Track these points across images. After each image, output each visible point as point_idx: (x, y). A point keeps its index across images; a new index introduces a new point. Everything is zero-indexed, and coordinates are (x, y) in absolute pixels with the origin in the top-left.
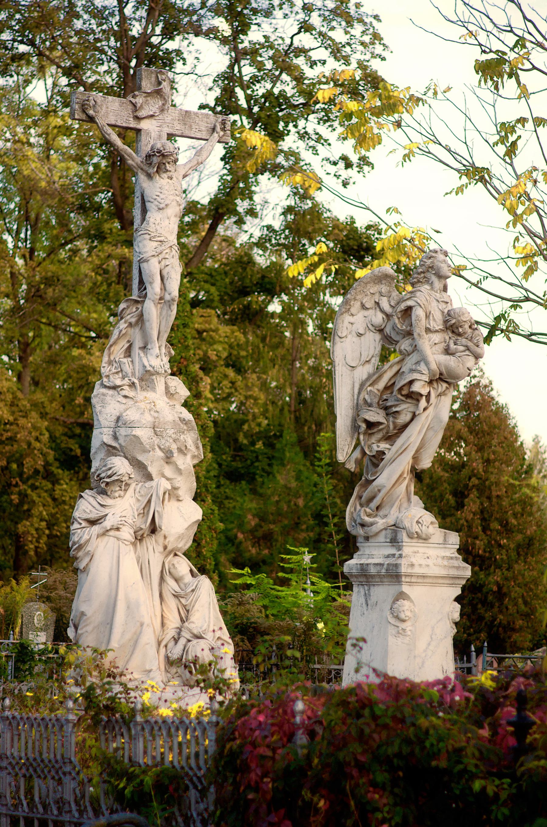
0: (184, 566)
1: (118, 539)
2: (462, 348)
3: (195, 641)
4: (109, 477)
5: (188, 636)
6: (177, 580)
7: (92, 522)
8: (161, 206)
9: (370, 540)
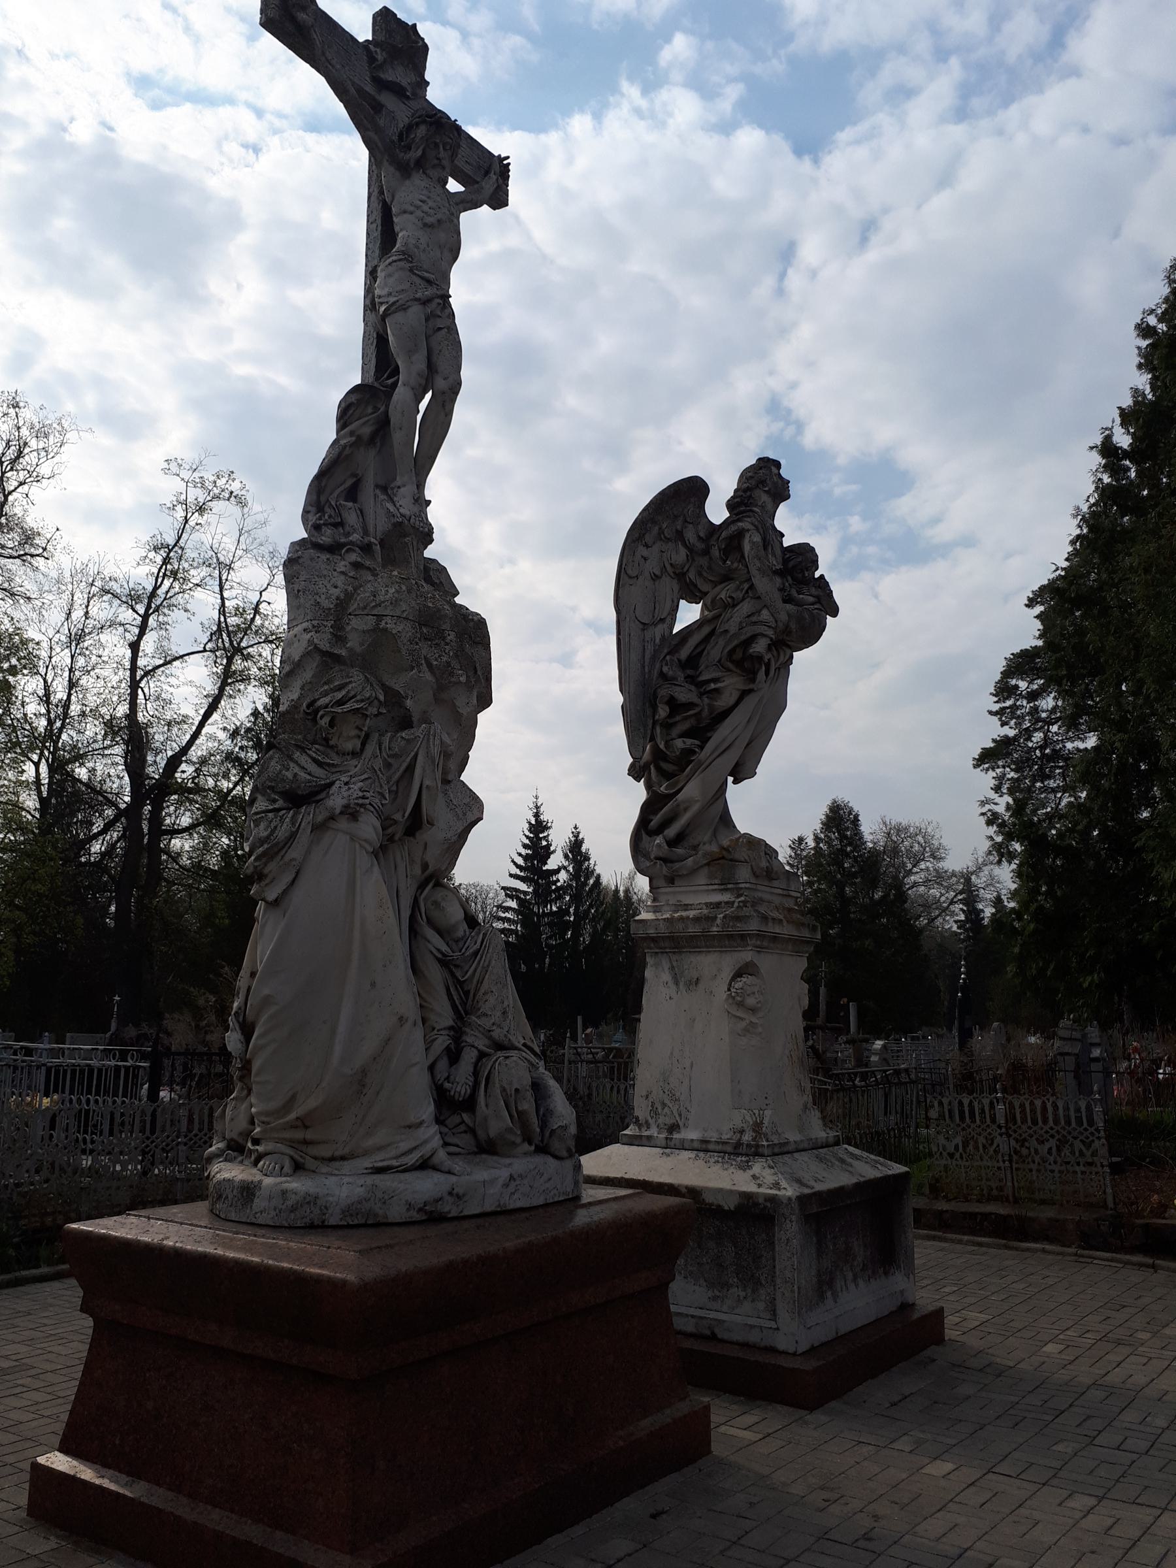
2: (811, 599)
5: (481, 1043)
6: (440, 933)
8: (429, 220)
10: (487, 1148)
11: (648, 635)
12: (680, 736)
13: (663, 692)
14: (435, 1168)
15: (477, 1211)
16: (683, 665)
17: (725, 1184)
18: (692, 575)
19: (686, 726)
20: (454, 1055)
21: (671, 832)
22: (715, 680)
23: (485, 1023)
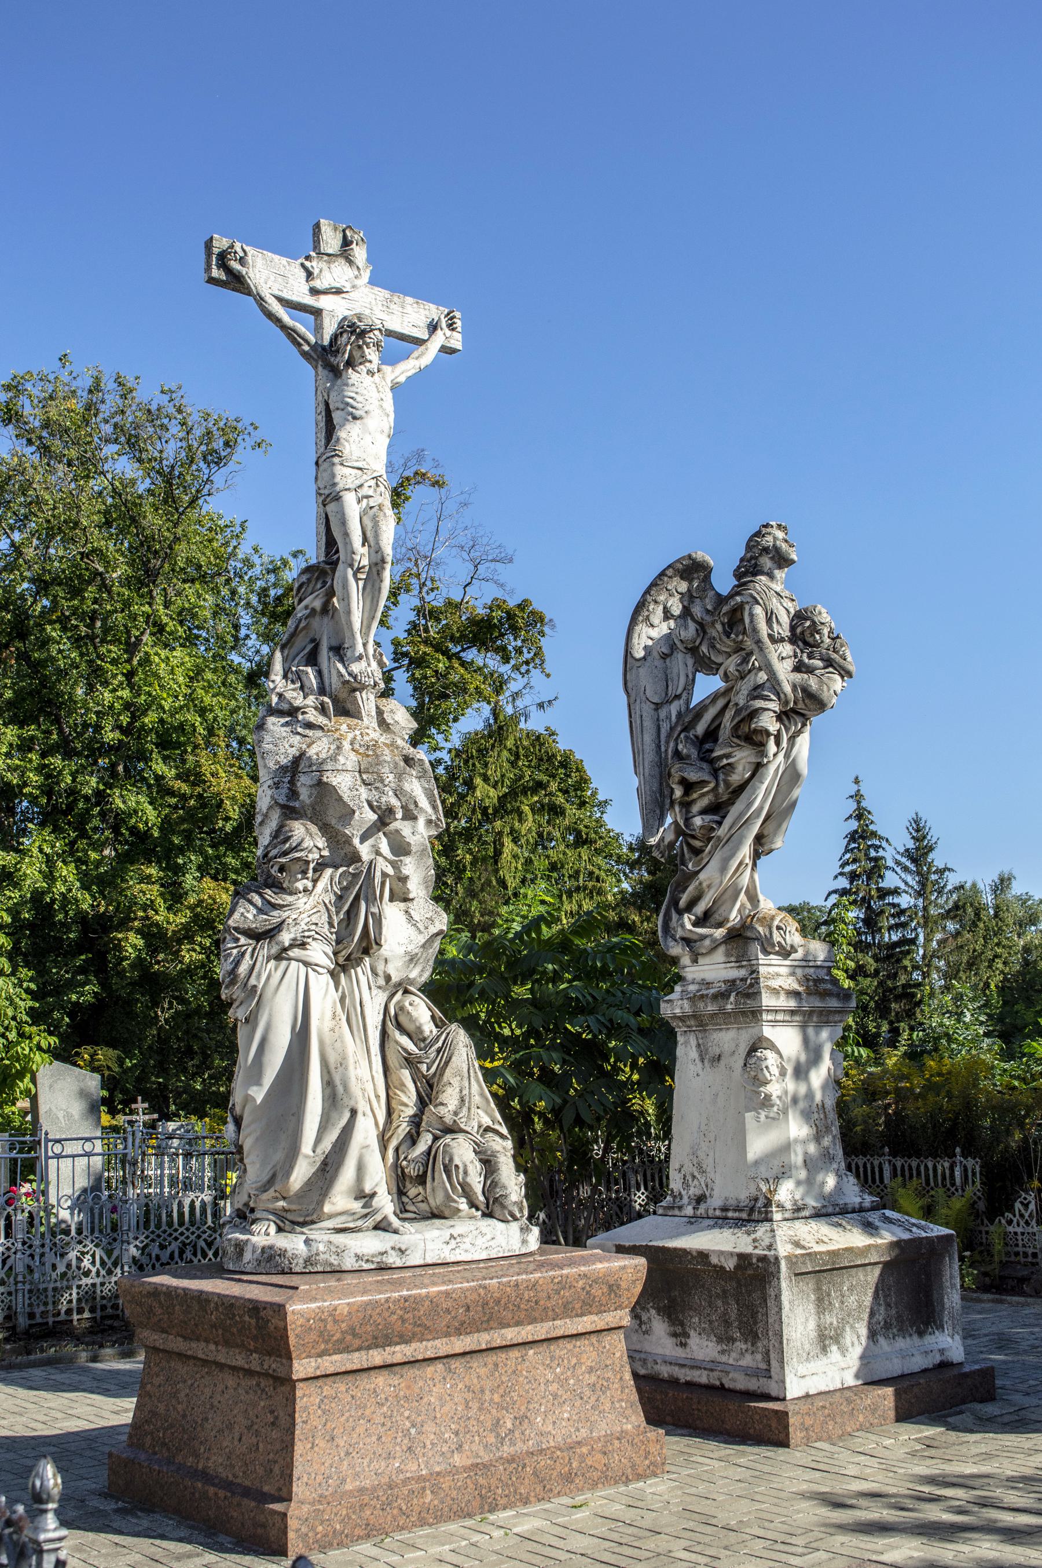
0: (421, 1012)
1: (306, 964)
3: (448, 1139)
4: (285, 854)
7: (257, 936)
9: (701, 961)
11: (663, 713)
12: (704, 812)
14: (385, 1230)
15: (421, 1262)
17: (727, 1248)
18: (704, 649)
19: (704, 802)
20: (412, 1139)
21: (700, 908)
22: (728, 756)
23: (442, 1111)
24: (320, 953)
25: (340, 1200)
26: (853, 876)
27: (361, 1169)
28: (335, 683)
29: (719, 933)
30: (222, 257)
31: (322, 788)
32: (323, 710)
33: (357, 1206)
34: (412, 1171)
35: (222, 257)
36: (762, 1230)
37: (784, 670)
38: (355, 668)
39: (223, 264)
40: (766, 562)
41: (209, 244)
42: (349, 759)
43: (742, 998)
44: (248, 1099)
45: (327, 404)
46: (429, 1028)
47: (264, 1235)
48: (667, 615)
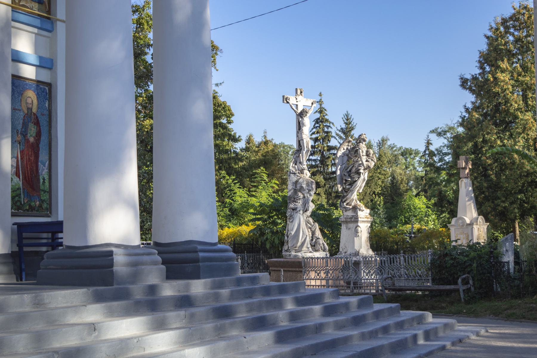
0: (311, 220)
10: (316, 251)
13: (344, 178)
16: (348, 172)
20: (312, 240)
24: (301, 212)
25: (304, 248)
26: (316, 140)
27: (307, 244)
28: (300, 169)
29: (351, 207)
30: (286, 98)
31: (302, 187)
32: (299, 173)
33: (307, 249)
34: (313, 244)
35: (286, 98)
36: (358, 257)
37: (364, 161)
38: (304, 166)
39: (286, 100)
40: (362, 141)
41: (283, 96)
42: (305, 182)
43: (355, 220)
44: (291, 233)
45: (299, 123)
46: (312, 224)
47: (293, 253)
48: (344, 149)
